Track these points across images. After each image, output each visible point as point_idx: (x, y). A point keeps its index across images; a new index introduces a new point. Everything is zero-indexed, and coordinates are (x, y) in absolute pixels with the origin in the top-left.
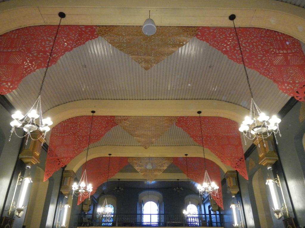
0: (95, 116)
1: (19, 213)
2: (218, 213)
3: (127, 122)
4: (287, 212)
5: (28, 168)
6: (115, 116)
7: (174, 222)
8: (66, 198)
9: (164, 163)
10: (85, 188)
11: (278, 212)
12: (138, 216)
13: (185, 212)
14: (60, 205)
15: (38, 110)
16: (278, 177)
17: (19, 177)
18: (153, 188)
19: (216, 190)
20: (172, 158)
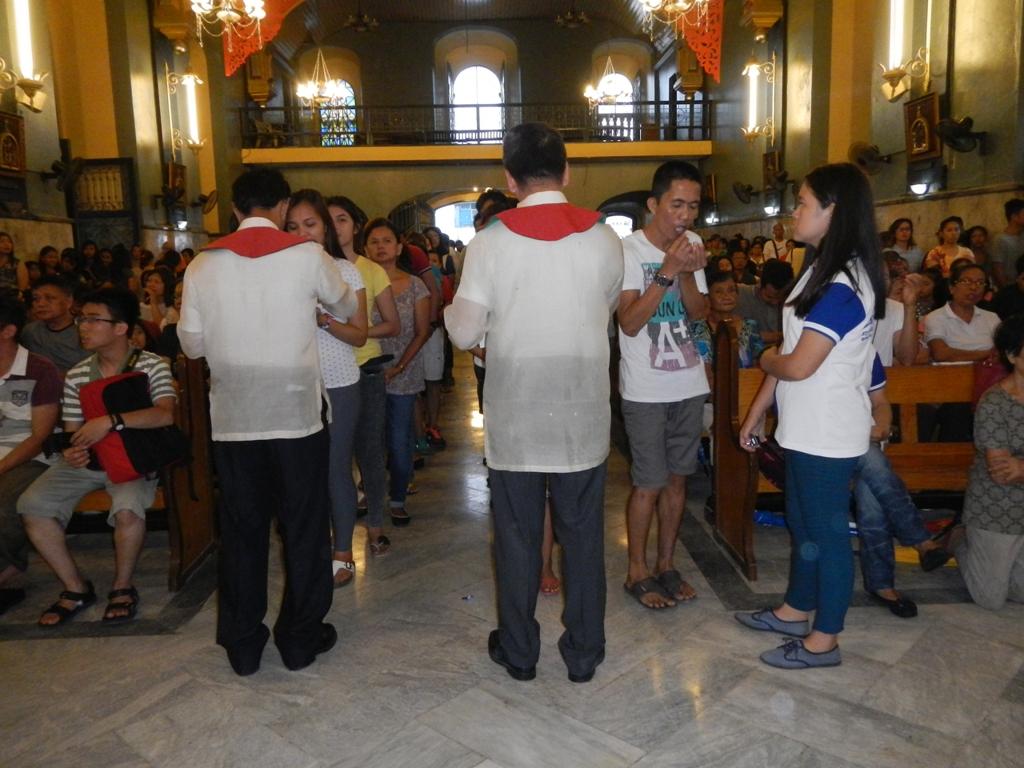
1: (31, 95)
2: (698, 96)
4: (927, 76)
8: (180, 51)
11: (894, 78)
12: (437, 113)
13: (590, 93)
14: (168, 76)
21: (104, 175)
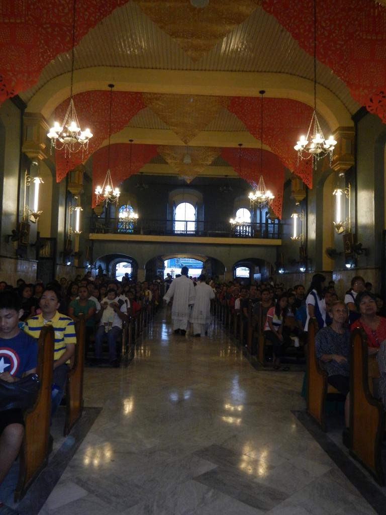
0: (114, 92)
3: (160, 103)
5: (35, 164)
6: (141, 93)
9: (208, 156)
10: (111, 193)
11: (339, 227)
13: (232, 221)
15: (76, 121)
16: (349, 186)
17: (26, 177)
19: (271, 199)
20: (221, 148)
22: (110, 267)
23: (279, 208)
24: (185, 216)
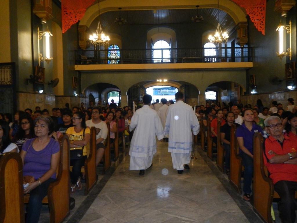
2: (245, 46)
7: (191, 58)
8: (44, 23)
14: (38, 33)
18: (165, 24)
21: (3, 70)
22: (103, 96)
23: (262, 22)
24: (161, 50)
